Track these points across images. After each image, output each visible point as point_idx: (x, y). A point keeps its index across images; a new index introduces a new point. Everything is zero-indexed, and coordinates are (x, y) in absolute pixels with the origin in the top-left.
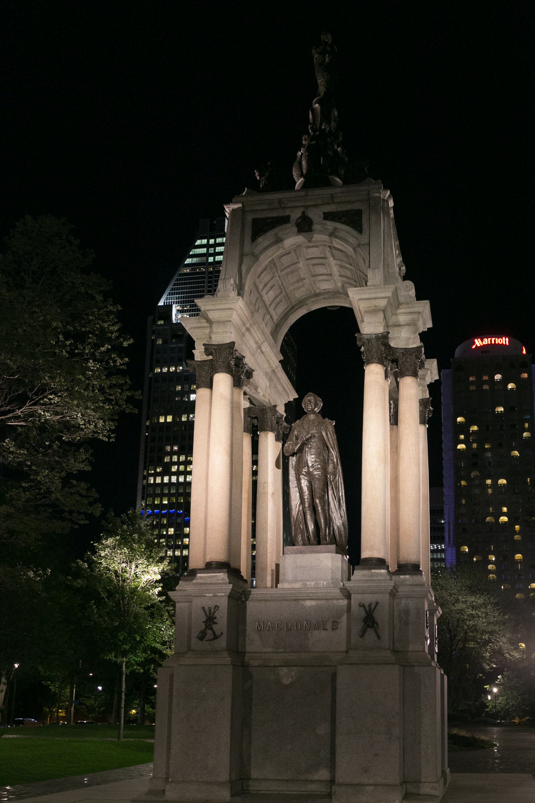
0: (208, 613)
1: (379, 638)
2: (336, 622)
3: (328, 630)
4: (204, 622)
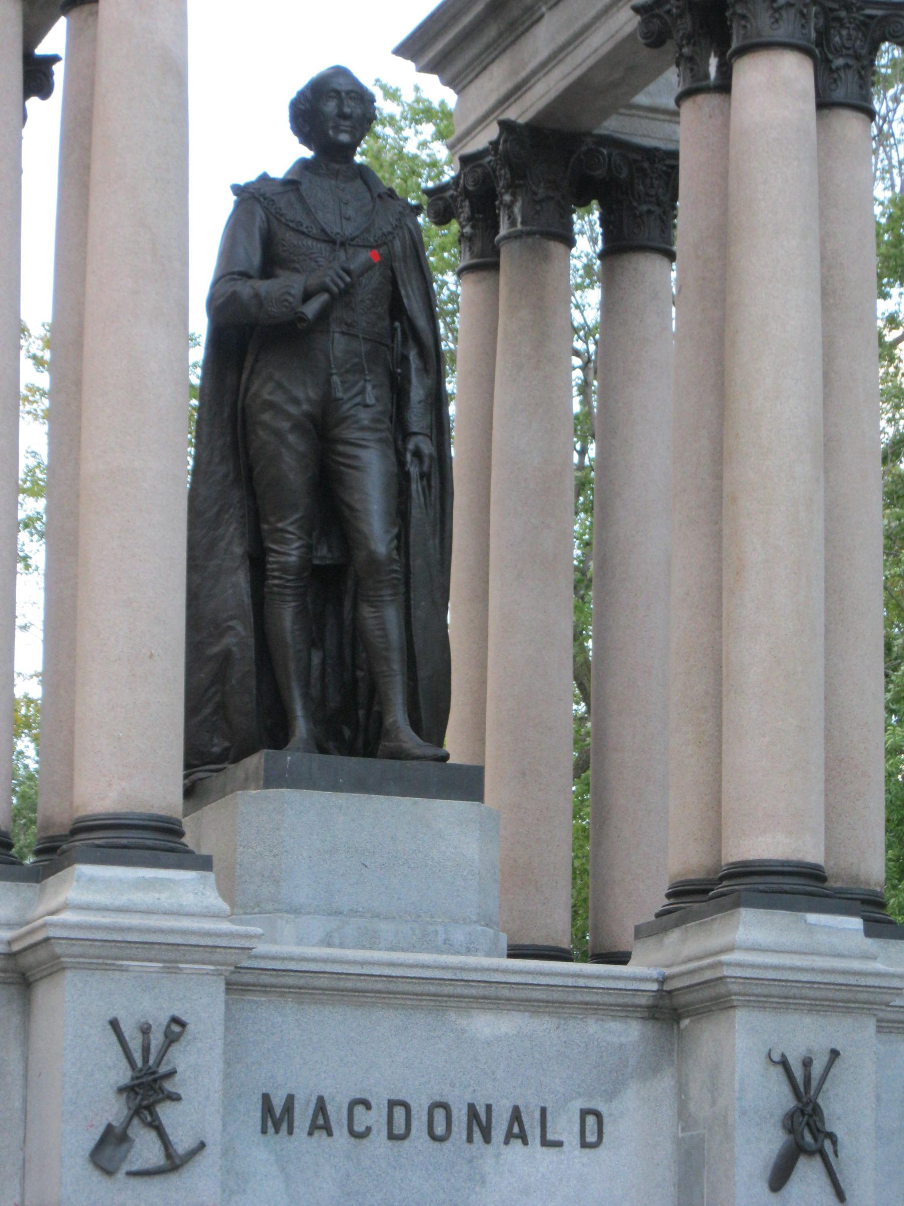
0: (135, 1046)
1: (840, 1195)
2: (598, 1115)
3: (566, 1147)
4: (121, 1090)
